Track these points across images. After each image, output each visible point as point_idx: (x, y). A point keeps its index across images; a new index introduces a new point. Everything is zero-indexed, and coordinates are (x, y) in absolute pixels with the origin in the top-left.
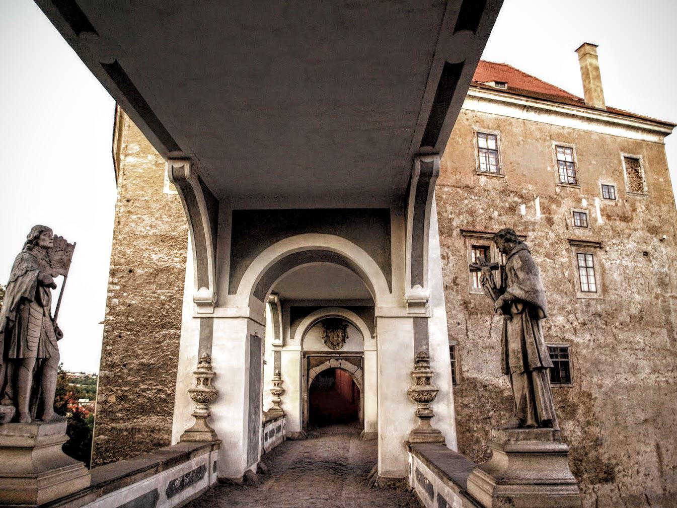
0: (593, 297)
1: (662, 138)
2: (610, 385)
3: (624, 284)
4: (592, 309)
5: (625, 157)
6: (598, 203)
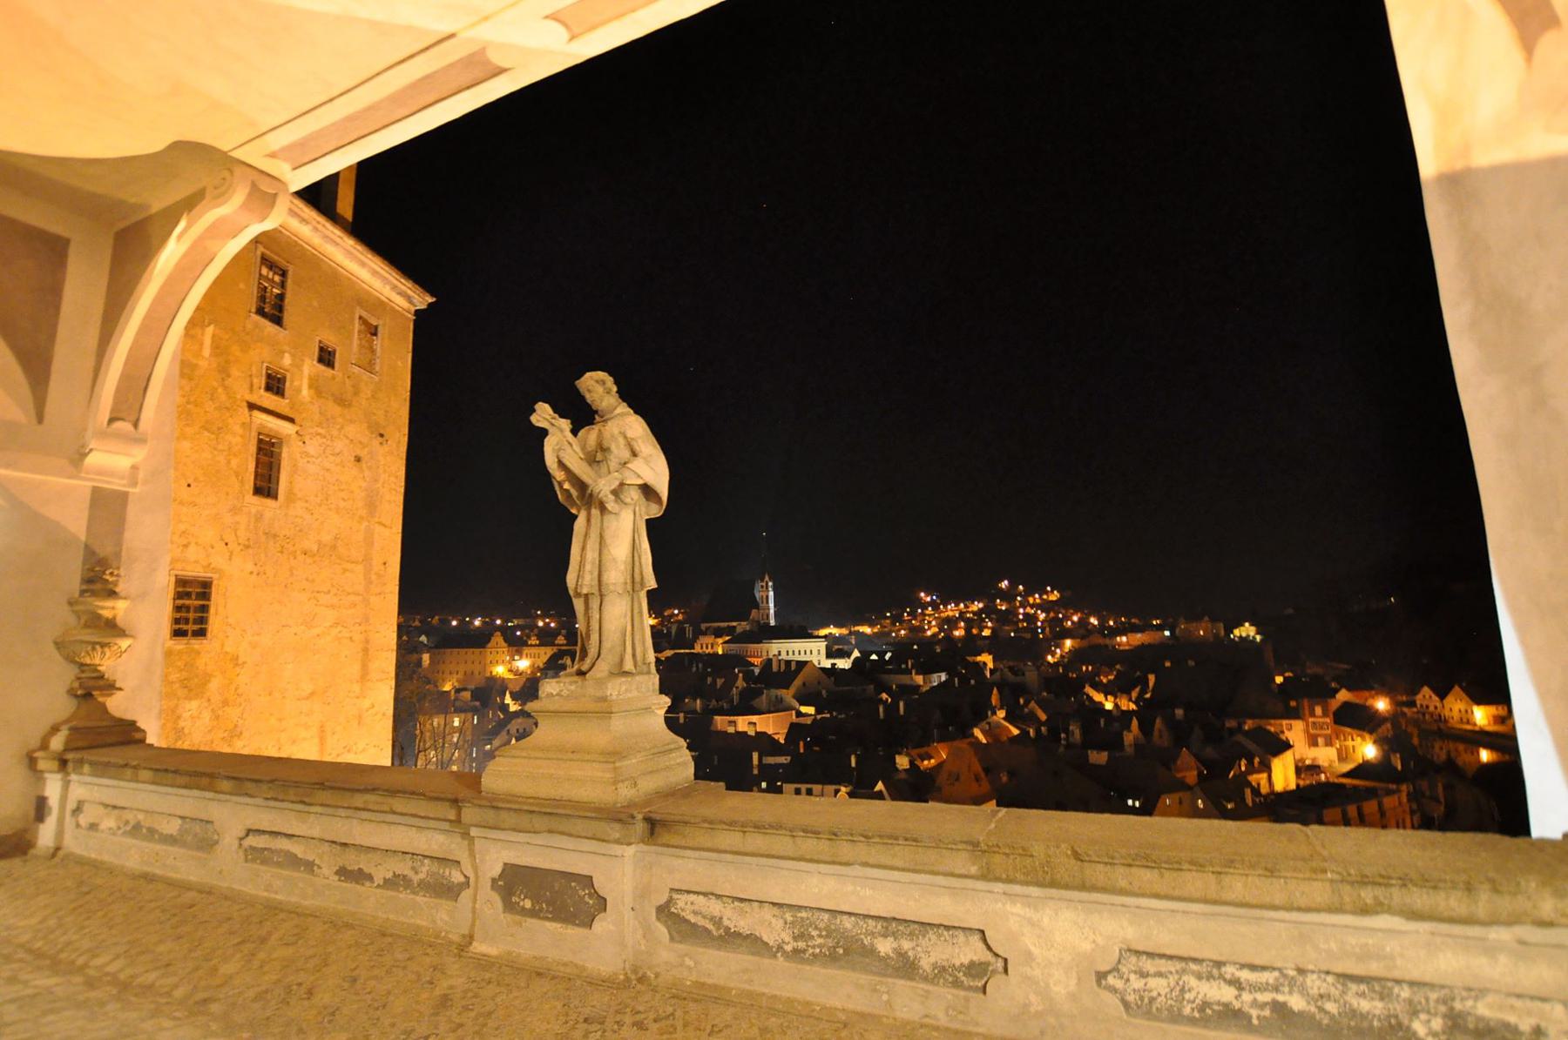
3: (319, 495)
5: (360, 318)
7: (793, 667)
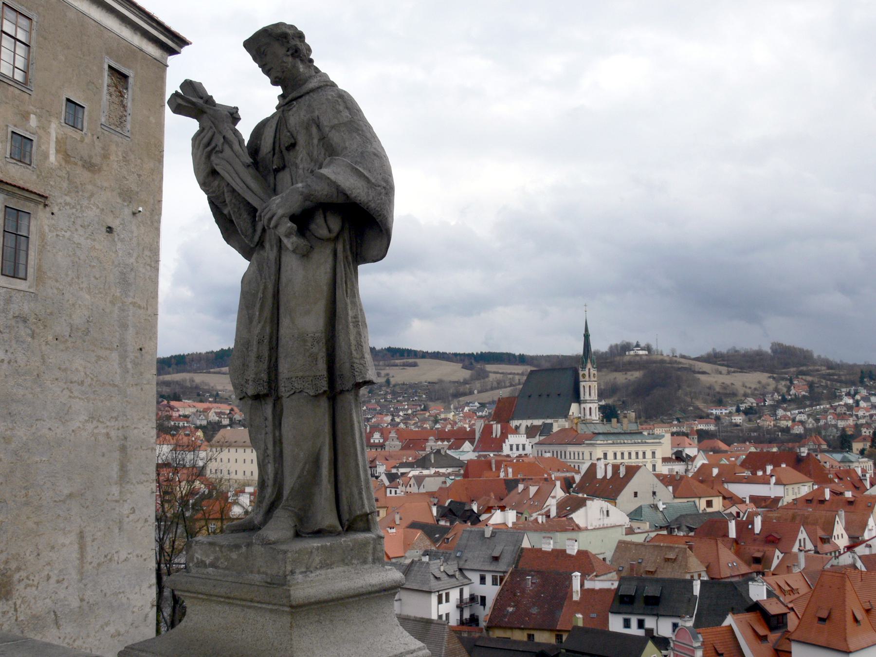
0: (18, 288)
1: (165, 54)
2: (25, 438)
4: (14, 308)
5: (110, 67)
6: (55, 129)
7: (622, 472)
